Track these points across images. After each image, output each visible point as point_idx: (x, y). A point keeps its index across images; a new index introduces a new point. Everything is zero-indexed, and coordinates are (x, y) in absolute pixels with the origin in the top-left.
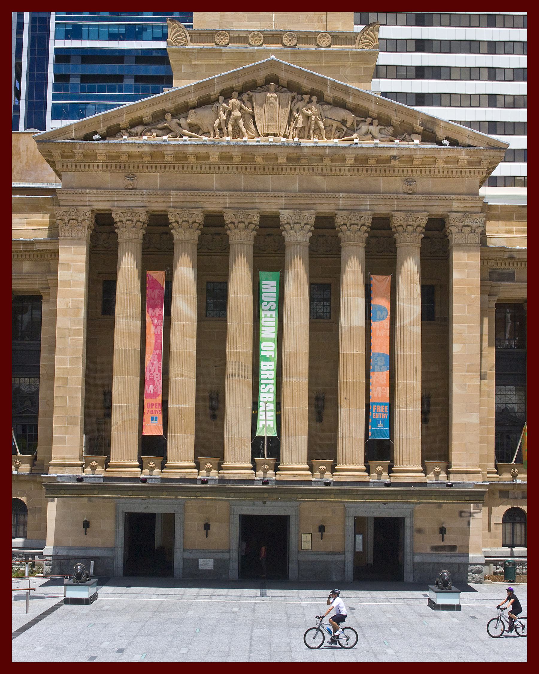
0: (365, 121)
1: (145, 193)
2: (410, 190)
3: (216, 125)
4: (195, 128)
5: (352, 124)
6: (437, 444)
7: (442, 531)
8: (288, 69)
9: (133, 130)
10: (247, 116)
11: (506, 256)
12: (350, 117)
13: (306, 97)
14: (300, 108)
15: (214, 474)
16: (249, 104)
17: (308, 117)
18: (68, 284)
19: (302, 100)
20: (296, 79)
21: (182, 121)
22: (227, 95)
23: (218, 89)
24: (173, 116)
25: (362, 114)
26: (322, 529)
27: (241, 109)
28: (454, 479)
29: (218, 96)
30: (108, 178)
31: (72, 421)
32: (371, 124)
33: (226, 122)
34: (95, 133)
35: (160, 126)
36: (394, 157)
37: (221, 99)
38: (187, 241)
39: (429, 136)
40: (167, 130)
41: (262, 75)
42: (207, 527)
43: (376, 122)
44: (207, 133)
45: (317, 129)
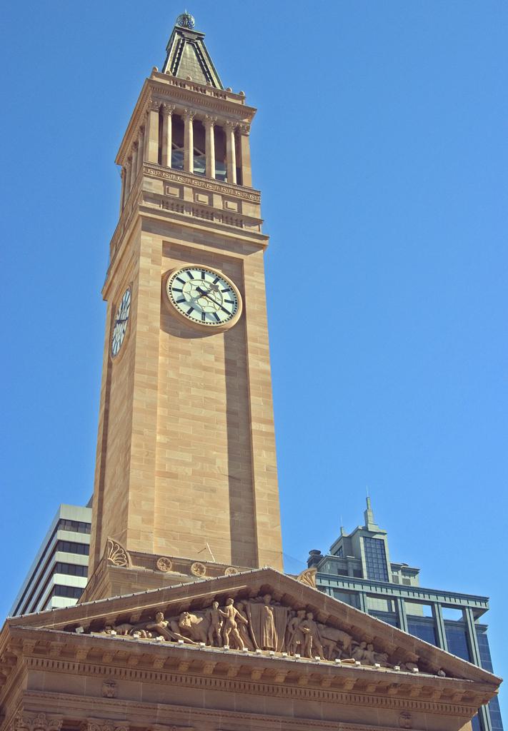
0: (358, 646)
1: (127, 704)
2: (408, 724)
8: (283, 579)
12: (347, 640)
13: (302, 613)
14: (297, 624)
19: (296, 616)
20: (291, 593)
25: (358, 638)
29: (213, 601)
30: (83, 681)
34: (77, 625)
35: (149, 627)
36: (395, 685)
39: (424, 667)
43: (371, 647)
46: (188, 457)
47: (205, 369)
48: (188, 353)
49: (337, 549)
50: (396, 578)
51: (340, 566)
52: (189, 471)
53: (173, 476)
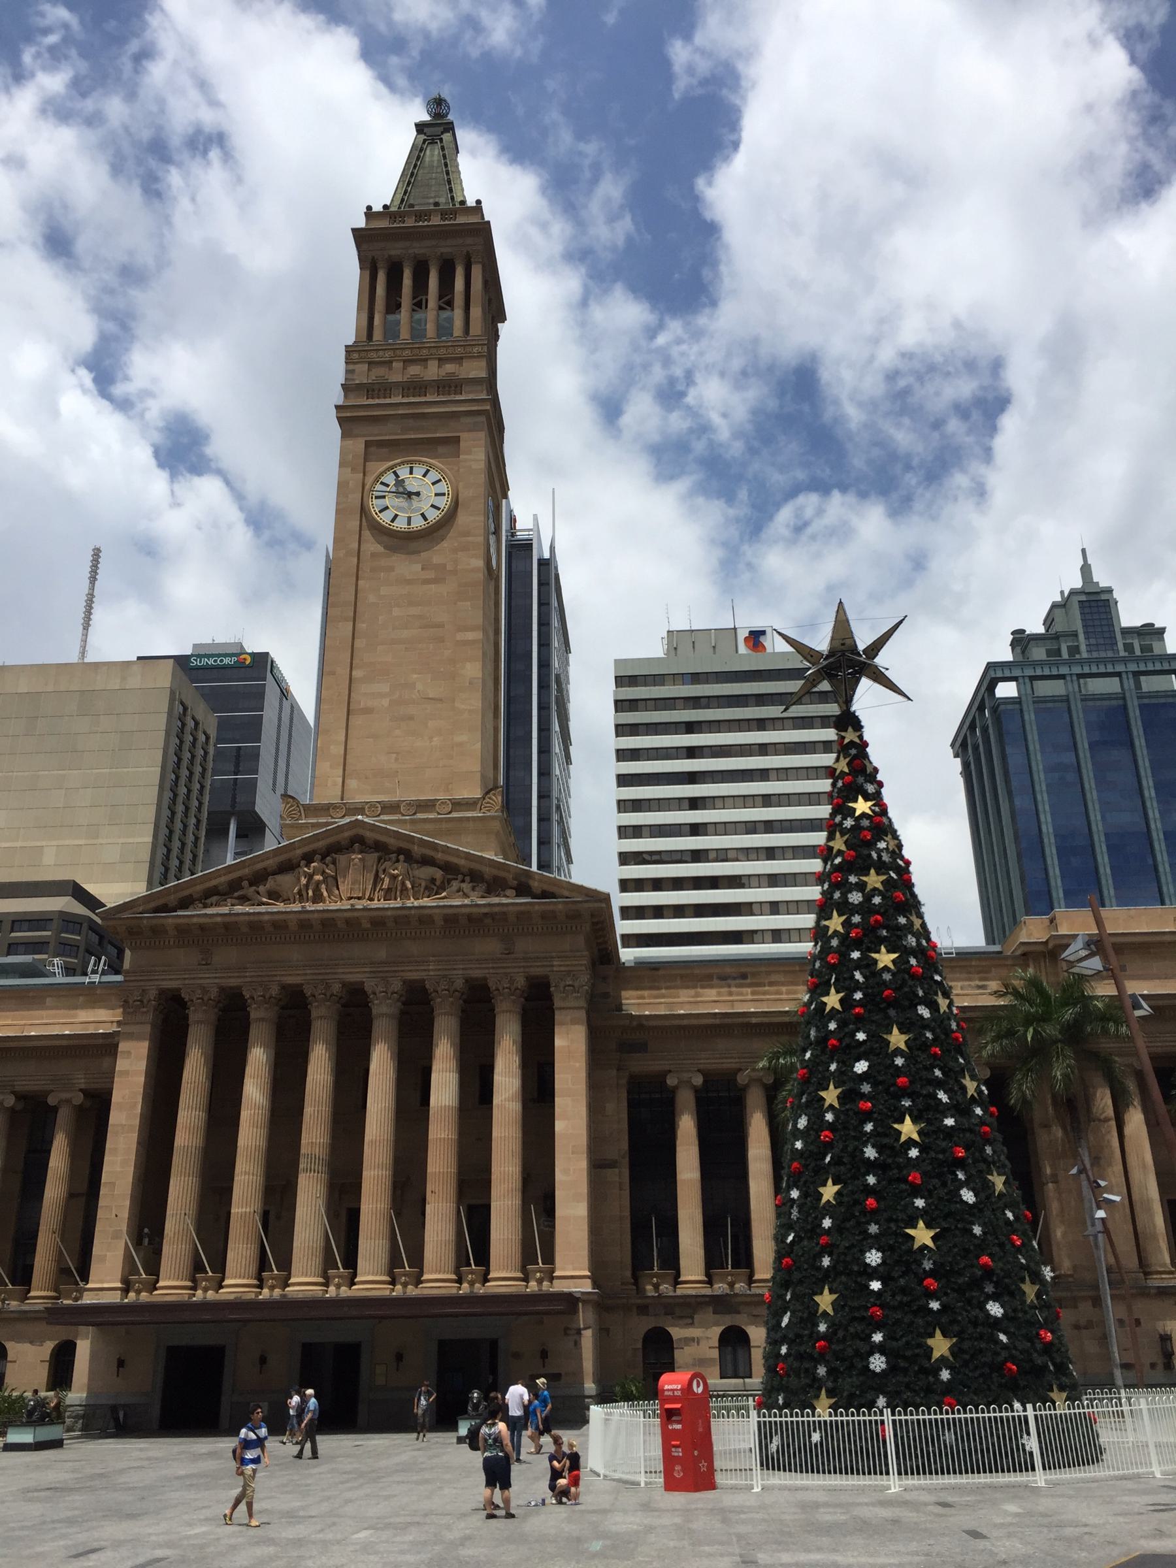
3: (296, 891)
4: (275, 895)
5: (443, 882)
6: (538, 1245)
7: (544, 1354)
9: (209, 901)
10: (330, 880)
11: (635, 1023)
12: (439, 874)
13: (393, 856)
15: (277, 1292)
16: (332, 866)
17: (394, 877)
18: (126, 1073)
19: (390, 859)
21: (261, 889)
22: (308, 858)
23: (299, 852)
24: (251, 885)
26: (399, 1357)
27: (323, 873)
28: (559, 1287)
31: (116, 1235)
32: (463, 881)
33: (307, 886)
37: (303, 863)
38: (262, 1019)
40: (244, 900)
41: (347, 834)
42: (263, 1360)
43: (468, 879)
44: (286, 900)
45: (404, 889)
46: (385, 688)
47: (409, 582)
48: (392, 569)
49: (1049, 621)
50: (1129, 647)
51: (1052, 646)
52: (385, 702)
53: (368, 711)
